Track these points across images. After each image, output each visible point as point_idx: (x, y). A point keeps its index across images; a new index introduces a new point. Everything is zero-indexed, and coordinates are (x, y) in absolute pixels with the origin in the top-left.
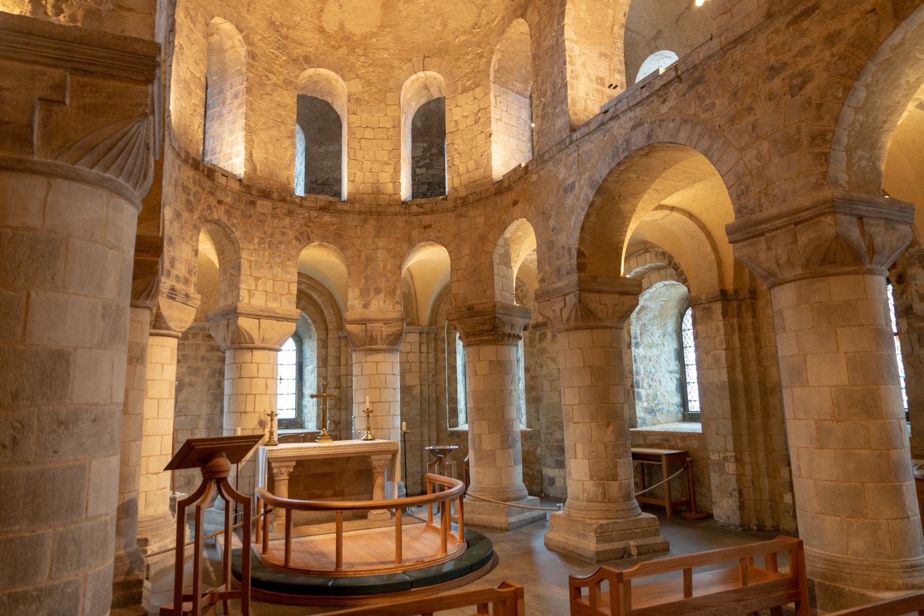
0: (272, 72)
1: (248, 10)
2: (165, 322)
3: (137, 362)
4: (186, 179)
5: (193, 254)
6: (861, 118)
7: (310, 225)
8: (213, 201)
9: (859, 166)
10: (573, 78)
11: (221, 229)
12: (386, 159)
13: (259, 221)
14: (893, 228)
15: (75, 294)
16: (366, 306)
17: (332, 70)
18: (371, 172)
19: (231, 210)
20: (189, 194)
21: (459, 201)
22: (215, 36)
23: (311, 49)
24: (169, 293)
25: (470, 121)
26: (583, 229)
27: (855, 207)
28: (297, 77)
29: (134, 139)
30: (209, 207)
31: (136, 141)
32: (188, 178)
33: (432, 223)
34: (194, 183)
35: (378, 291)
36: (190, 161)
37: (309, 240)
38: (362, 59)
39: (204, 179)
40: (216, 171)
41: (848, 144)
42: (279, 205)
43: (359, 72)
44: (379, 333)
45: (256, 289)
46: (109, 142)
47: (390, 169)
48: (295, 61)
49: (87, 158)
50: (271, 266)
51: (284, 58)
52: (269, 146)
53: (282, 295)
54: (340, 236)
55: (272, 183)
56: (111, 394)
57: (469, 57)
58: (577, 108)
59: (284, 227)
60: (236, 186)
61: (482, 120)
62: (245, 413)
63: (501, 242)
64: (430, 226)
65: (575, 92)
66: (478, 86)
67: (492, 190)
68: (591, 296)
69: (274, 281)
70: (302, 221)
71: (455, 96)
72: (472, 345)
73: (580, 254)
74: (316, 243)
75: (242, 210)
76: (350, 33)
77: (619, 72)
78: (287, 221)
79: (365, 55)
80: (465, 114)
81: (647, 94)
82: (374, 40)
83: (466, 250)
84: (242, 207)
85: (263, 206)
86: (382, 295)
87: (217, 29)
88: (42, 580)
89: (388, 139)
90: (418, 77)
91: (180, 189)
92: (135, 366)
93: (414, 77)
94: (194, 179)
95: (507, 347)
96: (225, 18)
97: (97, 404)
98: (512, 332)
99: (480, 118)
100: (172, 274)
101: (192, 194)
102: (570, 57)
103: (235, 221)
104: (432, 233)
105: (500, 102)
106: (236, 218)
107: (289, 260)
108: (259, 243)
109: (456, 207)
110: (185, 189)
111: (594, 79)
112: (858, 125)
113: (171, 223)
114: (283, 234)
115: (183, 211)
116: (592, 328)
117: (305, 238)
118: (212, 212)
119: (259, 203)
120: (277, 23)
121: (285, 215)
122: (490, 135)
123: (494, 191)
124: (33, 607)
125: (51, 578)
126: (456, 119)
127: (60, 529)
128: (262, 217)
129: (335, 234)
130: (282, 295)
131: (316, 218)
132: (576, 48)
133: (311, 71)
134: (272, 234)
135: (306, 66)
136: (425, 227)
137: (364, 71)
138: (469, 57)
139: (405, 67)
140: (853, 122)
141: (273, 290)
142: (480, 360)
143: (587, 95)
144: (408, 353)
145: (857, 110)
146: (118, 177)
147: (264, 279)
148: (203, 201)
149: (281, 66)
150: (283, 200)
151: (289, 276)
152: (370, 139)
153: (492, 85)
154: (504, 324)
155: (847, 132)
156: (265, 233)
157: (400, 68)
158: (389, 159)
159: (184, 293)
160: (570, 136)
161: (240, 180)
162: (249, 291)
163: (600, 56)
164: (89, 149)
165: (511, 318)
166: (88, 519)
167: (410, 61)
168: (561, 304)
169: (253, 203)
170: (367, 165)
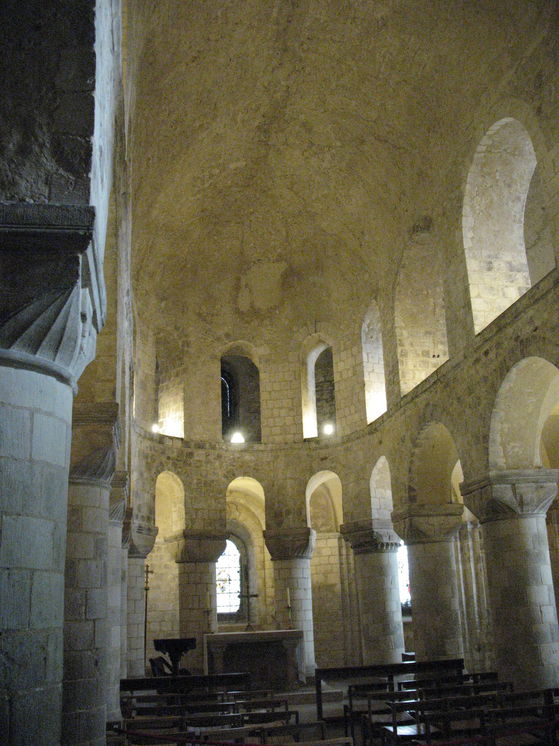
2: (136, 549)
6: (506, 426)
7: (234, 464)
9: (513, 452)
10: (402, 355)
11: (170, 476)
13: (197, 467)
14: (542, 487)
18: (279, 416)
24: (138, 529)
25: (350, 373)
26: (410, 471)
30: (161, 463)
32: (147, 447)
33: (327, 455)
34: (151, 450)
38: (269, 328)
48: (218, 339)
54: (258, 470)
55: (205, 436)
58: (407, 378)
60: (179, 444)
63: (375, 471)
64: (326, 458)
65: (404, 366)
67: (366, 431)
70: (229, 462)
71: (340, 353)
72: (361, 553)
73: (411, 489)
76: (259, 309)
77: (442, 343)
78: (217, 464)
79: (272, 325)
80: (347, 368)
81: (429, 386)
82: (277, 312)
83: (352, 478)
84: (184, 458)
85: (199, 455)
95: (394, 553)
98: (391, 541)
100: (139, 516)
101: (149, 458)
102: (400, 340)
103: (180, 470)
104: (327, 463)
105: (372, 357)
106: (180, 468)
109: (343, 443)
110: (146, 457)
111: (420, 352)
112: (506, 430)
116: (424, 543)
117: (231, 475)
119: (195, 454)
121: (215, 459)
122: (364, 385)
123: (367, 432)
128: (198, 464)
129: (254, 469)
131: (239, 458)
132: (405, 333)
134: (206, 475)
135: (227, 341)
136: (322, 459)
140: (502, 429)
143: (415, 367)
144: (329, 556)
150: (214, 448)
153: (363, 345)
154: (381, 536)
160: (400, 402)
161: (182, 439)
162: (191, 520)
163: (426, 334)
165: (388, 531)
168: (403, 526)
169: (191, 455)
170: (276, 412)
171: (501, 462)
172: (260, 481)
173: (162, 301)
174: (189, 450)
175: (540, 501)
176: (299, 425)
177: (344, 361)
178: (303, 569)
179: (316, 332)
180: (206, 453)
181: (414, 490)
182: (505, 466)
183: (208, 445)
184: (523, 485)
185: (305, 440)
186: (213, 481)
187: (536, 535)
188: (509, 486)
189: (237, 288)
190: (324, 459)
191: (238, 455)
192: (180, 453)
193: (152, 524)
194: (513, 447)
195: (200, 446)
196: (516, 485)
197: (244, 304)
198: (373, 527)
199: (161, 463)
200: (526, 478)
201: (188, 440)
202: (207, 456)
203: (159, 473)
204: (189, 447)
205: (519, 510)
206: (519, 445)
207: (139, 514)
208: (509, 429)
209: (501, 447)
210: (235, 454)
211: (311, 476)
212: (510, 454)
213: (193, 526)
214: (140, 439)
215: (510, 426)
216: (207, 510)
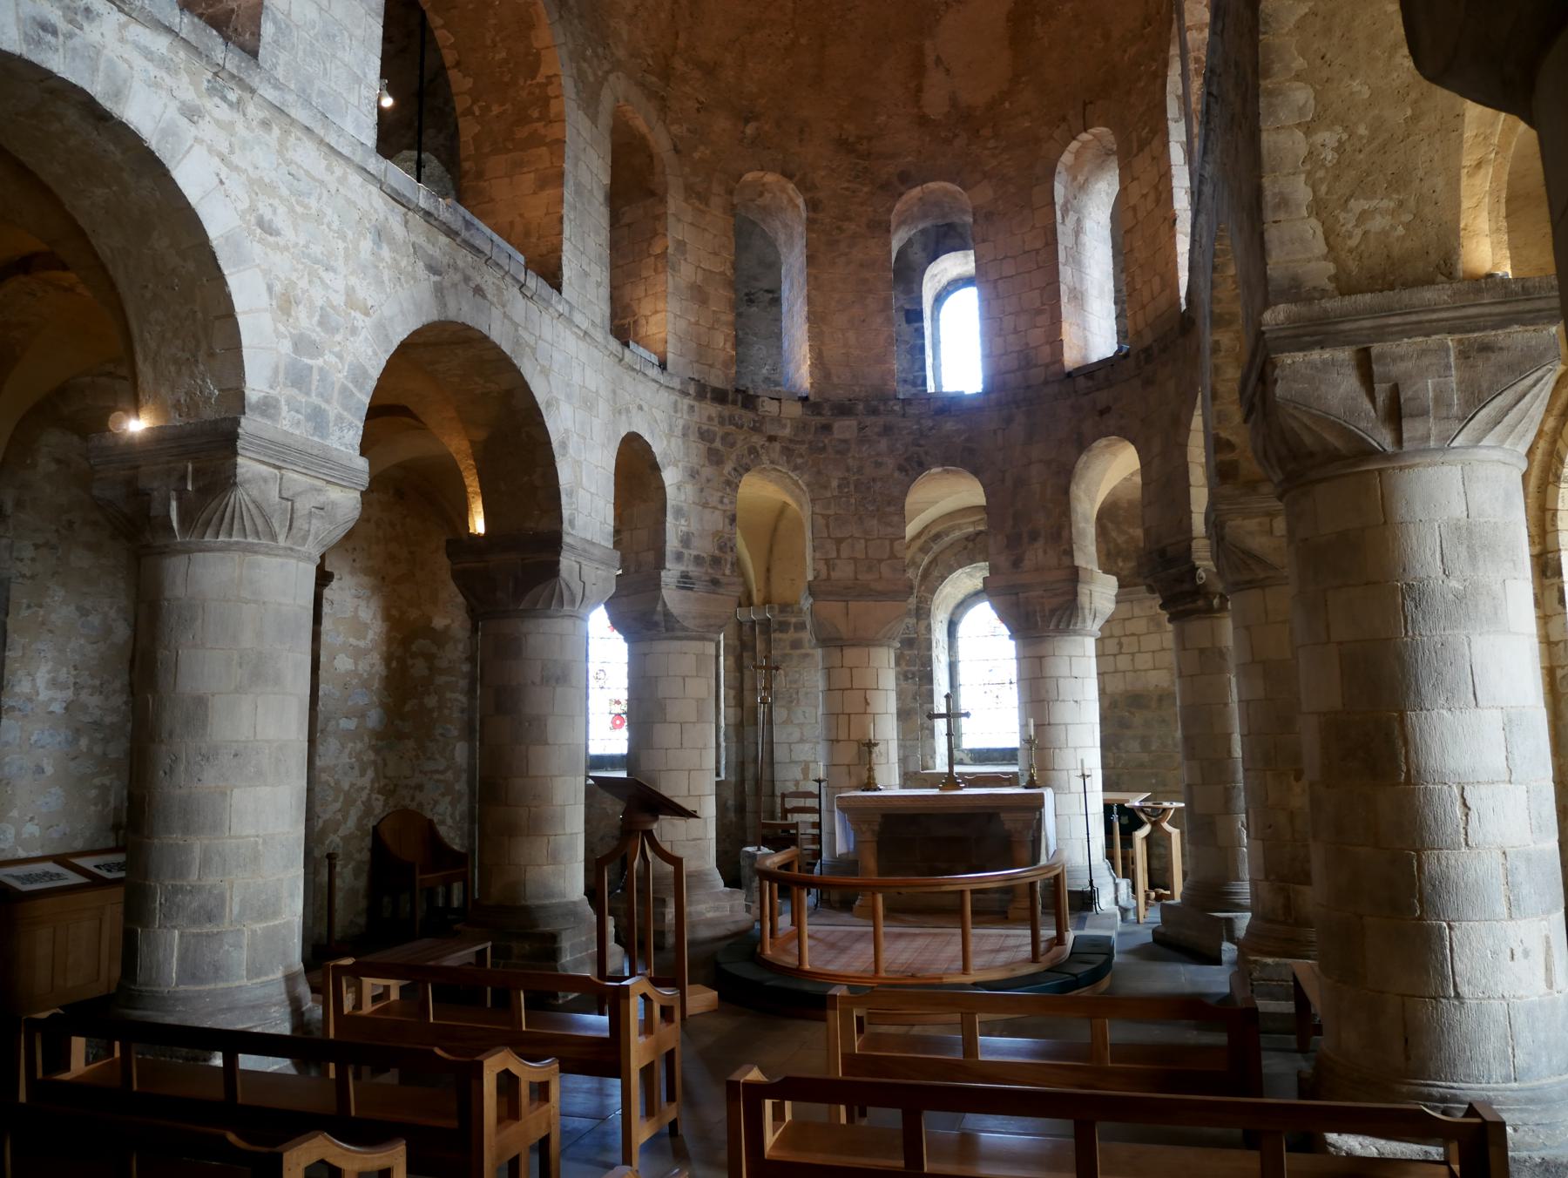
0: (849, 219)
1: (801, 141)
3: (557, 683)
4: (705, 420)
5: (727, 521)
6: (1327, 138)
7: (922, 442)
8: (758, 440)
9: (1365, 233)
12: (1038, 304)
13: (838, 452)
14: (1486, 348)
15: (211, 648)
16: (1017, 563)
17: (945, 180)
18: (1016, 331)
19: (792, 446)
20: (712, 441)
21: (1142, 356)
22: (766, 194)
23: (910, 159)
24: (679, 582)
27: (1331, 328)
28: (890, 211)
29: (237, 505)
30: (753, 450)
31: (241, 508)
32: (710, 418)
34: (722, 423)
35: (1034, 537)
36: (709, 395)
37: (922, 467)
39: (738, 411)
40: (758, 397)
41: (1316, 199)
42: (869, 420)
43: (986, 168)
44: (1038, 608)
45: (838, 557)
46: (218, 514)
47: (1043, 320)
48: (885, 187)
49: (209, 532)
50: (860, 518)
51: (866, 189)
52: (851, 335)
53: (880, 561)
56: (255, 732)
57: (1142, 84)
59: (878, 454)
60: (796, 410)
61: (1164, 196)
62: (838, 741)
66: (1154, 132)
68: (1252, 524)
69: (867, 540)
74: (934, 470)
75: (810, 443)
78: (883, 444)
82: (1007, 105)
85: (845, 428)
86: (1040, 544)
87: (763, 185)
88: (193, 877)
89: (1039, 268)
90: (1084, 145)
91: (693, 437)
92: (554, 688)
93: (1074, 145)
94: (721, 416)
96: (762, 170)
97: (236, 741)
99: (1160, 194)
101: (718, 439)
103: (799, 461)
106: (801, 456)
107: (889, 504)
108: (839, 486)
110: (704, 436)
112: (1329, 156)
113: (679, 489)
114: (878, 465)
115: (703, 466)
118: (758, 455)
119: (836, 426)
120: (851, 139)
121: (879, 434)
122: (1175, 220)
124: (188, 898)
125: (199, 878)
126: (1131, 204)
127: (206, 842)
130: (880, 561)
133: (916, 192)
134: (860, 470)
136: (1102, 413)
137: (994, 163)
138: (1142, 84)
139: (1057, 134)
140: (1311, 153)
141: (866, 553)
142: (1184, 649)
145: (1308, 129)
146: (245, 536)
147: (850, 540)
148: (739, 443)
149: (862, 204)
150: (874, 412)
151: (890, 530)
152: (1012, 276)
155: (1303, 177)
156: (848, 470)
157: (1051, 137)
158: (1043, 304)
159: (707, 578)
162: (827, 561)
164: (208, 524)
166: (230, 837)
167: (1064, 119)
169: (827, 428)
171: (1320, 271)
172: (976, 472)
173: (747, 121)
174: (819, 420)
175: (1475, 400)
176: (1056, 343)
177: (1138, 178)
178: (1070, 657)
179: (1085, 130)
180: (859, 423)
181: (1229, 446)
182: (1330, 286)
183: (861, 407)
184: (1405, 345)
185: (1069, 375)
186: (874, 480)
187: (1458, 528)
188: (1345, 354)
189: (918, 69)
190: (1104, 412)
191: (930, 423)
192: (801, 427)
193: (728, 572)
194: (1363, 217)
195: (843, 410)
196: (1376, 349)
197: (935, 102)
198: (1194, 556)
199: (753, 450)
200: (1414, 318)
201: (818, 400)
202: (861, 429)
203: (747, 470)
204: (819, 414)
205: (1383, 438)
206: (1385, 204)
207: (685, 551)
208: (1340, 148)
209: (1314, 222)
210: (923, 421)
211: (1080, 453)
212: (1353, 243)
213: (832, 574)
214: (687, 401)
215: (1345, 136)
216: (862, 541)
